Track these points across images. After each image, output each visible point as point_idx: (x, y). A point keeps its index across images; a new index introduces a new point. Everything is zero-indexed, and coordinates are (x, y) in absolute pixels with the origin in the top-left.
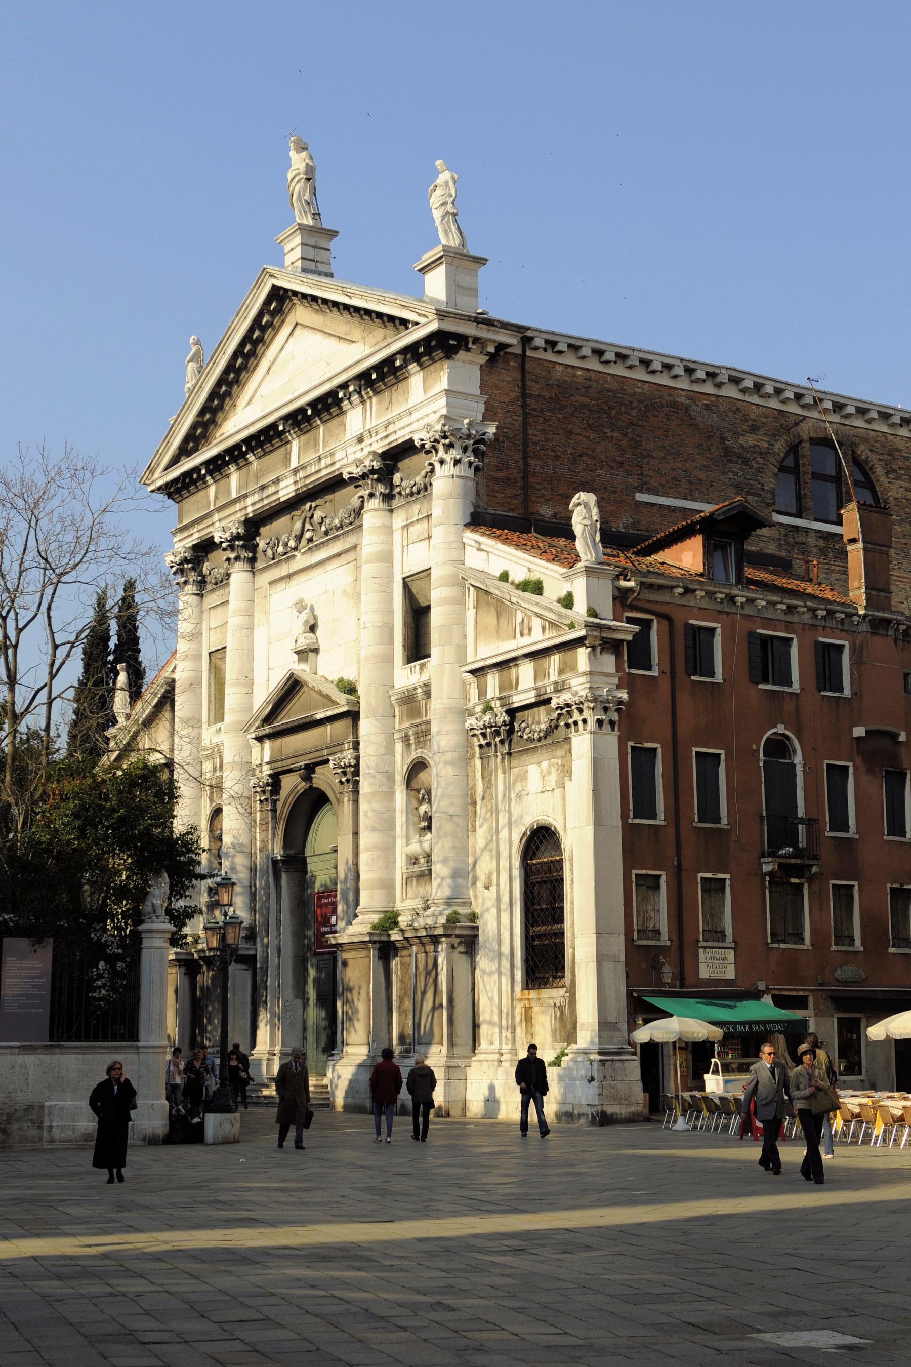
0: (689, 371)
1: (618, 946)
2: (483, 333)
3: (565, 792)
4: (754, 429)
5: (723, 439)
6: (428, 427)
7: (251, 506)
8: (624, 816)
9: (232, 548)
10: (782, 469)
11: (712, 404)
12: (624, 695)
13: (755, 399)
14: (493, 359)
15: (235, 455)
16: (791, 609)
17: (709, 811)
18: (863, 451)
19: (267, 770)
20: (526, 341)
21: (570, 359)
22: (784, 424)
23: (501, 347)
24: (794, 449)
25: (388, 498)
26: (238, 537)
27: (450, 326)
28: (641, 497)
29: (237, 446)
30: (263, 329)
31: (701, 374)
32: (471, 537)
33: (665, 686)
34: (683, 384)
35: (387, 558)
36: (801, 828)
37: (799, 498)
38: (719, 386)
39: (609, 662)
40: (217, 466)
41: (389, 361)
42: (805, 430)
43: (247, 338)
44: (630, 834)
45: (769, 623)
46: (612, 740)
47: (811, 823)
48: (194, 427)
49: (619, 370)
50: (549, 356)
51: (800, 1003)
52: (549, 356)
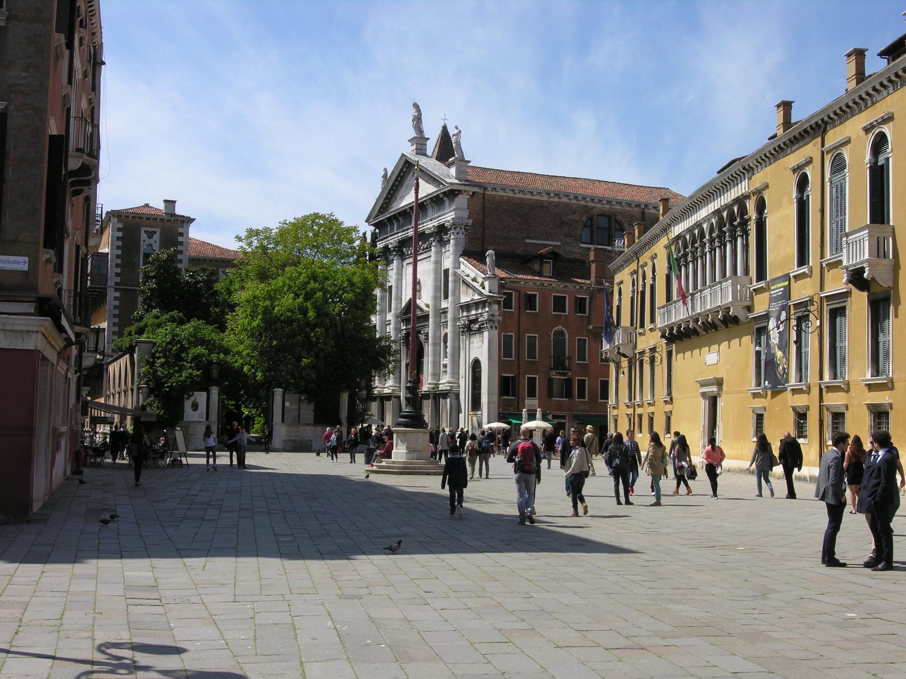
0: (549, 194)
1: (495, 398)
2: (467, 188)
3: (480, 348)
4: (574, 213)
5: (561, 218)
6: (449, 221)
7: (401, 236)
8: (499, 357)
9: (394, 250)
10: (585, 226)
11: (557, 205)
12: (500, 318)
13: (574, 201)
14: (472, 196)
15: (395, 217)
16: (565, 286)
17: (532, 354)
18: (619, 218)
19: (404, 332)
20: (485, 189)
21: (501, 193)
22: (587, 210)
23: (474, 193)
24: (591, 219)
25: (439, 241)
26: (396, 247)
27: (454, 187)
28: (527, 241)
29: (395, 215)
30: (404, 173)
31: (552, 195)
32: (461, 259)
33: (516, 314)
34: (545, 198)
35: (438, 263)
36: (567, 361)
37: (592, 237)
38: (560, 198)
39: (496, 307)
40: (390, 220)
41: (438, 196)
42: (595, 212)
43: (399, 175)
44: (501, 363)
45: (557, 291)
46: (495, 333)
47: (569, 358)
48: (383, 204)
49: (521, 196)
50: (494, 193)
51: (563, 417)
52: (494, 193)
